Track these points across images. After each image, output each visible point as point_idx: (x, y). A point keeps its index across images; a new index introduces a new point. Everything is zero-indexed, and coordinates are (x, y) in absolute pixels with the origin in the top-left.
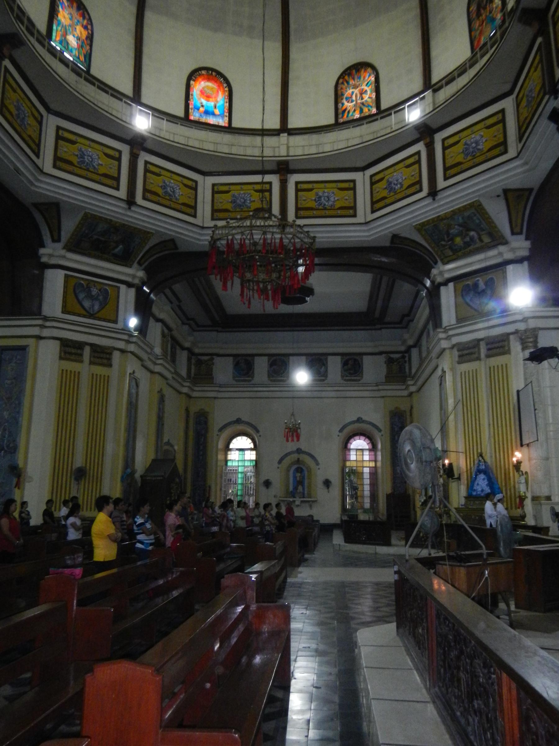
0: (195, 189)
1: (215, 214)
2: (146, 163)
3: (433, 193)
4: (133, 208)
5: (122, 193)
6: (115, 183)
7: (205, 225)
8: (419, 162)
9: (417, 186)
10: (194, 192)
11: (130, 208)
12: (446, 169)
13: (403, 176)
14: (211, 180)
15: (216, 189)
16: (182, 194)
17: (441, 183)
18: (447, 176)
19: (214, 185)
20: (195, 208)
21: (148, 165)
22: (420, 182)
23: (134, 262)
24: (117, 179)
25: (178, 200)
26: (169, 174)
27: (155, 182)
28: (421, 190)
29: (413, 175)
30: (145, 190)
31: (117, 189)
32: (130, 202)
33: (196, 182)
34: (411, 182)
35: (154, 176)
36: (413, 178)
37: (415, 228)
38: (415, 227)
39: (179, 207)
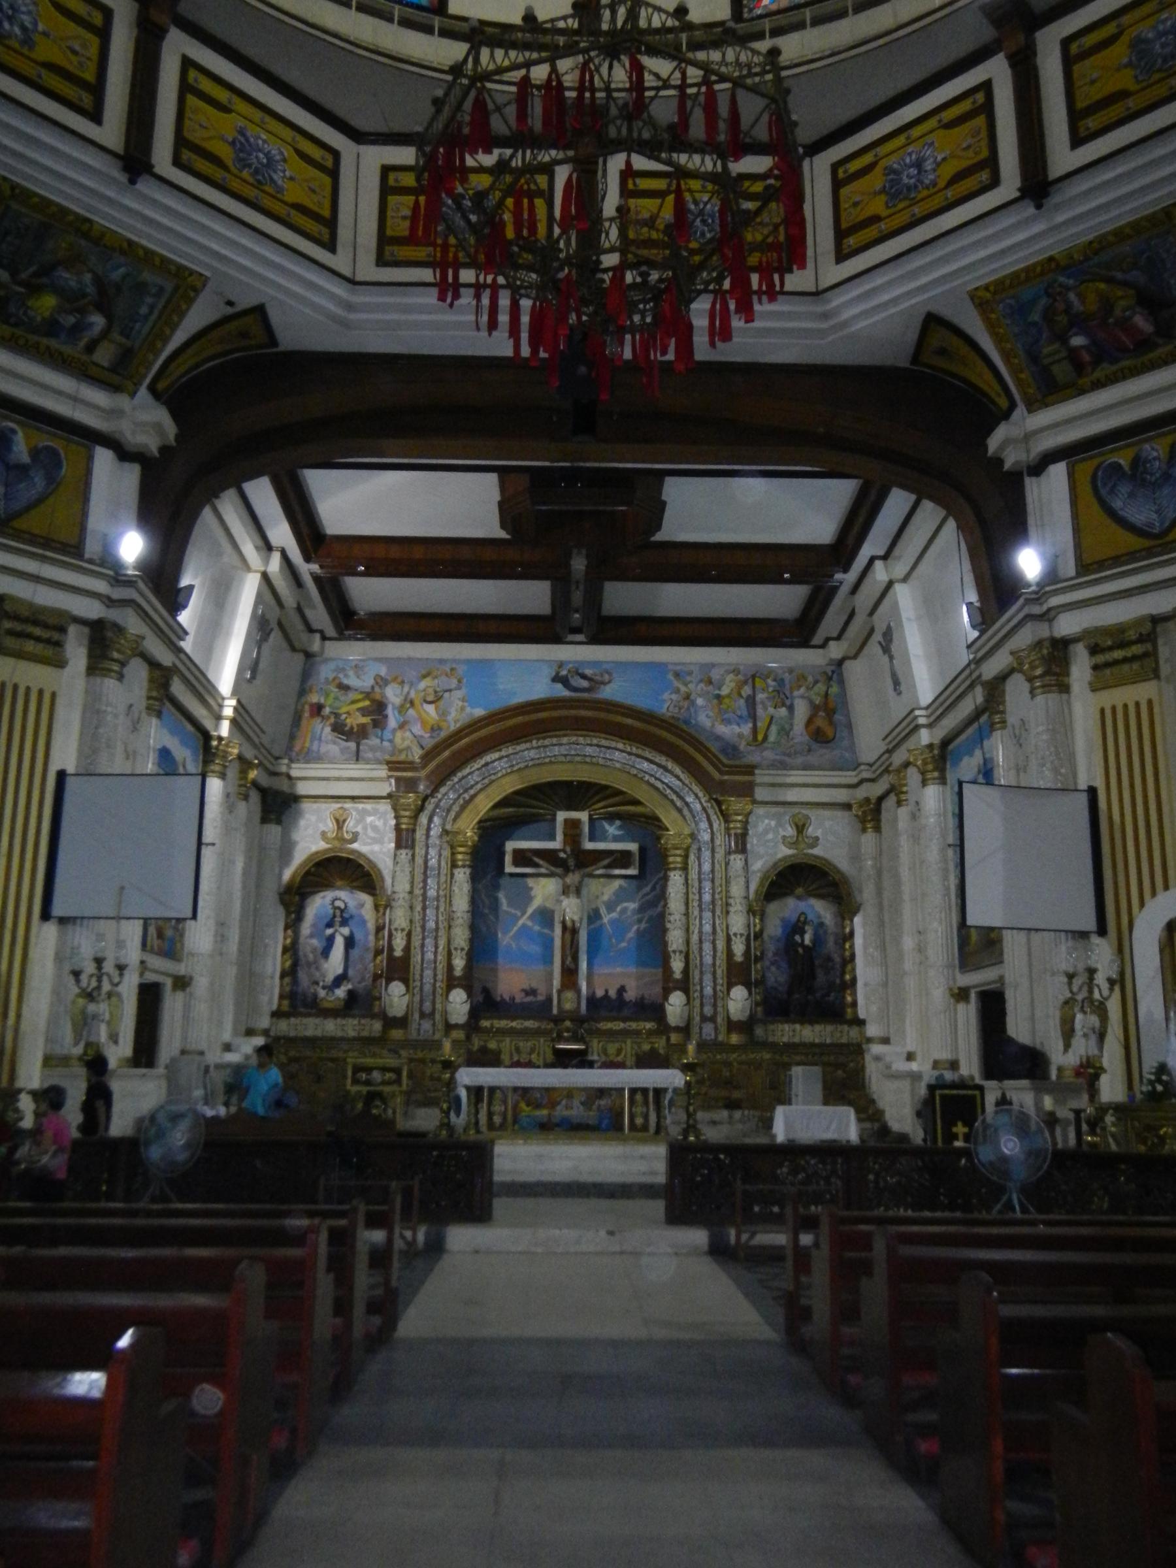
0: (334, 174)
1: (388, 249)
2: (187, 63)
3: (1038, 187)
4: (145, 186)
5: (111, 131)
6: (87, 100)
7: (360, 277)
8: (988, 109)
9: (984, 176)
10: (327, 180)
11: (132, 182)
12: (1075, 116)
13: (943, 153)
14: (377, 156)
15: (391, 182)
16: (295, 182)
17: (1062, 157)
18: (1083, 133)
19: (386, 170)
20: (331, 223)
21: (192, 74)
22: (991, 162)
23: (137, 385)
24: (97, 89)
25: (280, 190)
26: (257, 115)
27: (216, 129)
28: (995, 182)
29: (969, 147)
30: (181, 141)
31: (96, 117)
32: (135, 162)
33: (336, 154)
34: (965, 164)
35: (210, 110)
36: (970, 153)
37: (972, 298)
38: (973, 295)
39: (282, 210)
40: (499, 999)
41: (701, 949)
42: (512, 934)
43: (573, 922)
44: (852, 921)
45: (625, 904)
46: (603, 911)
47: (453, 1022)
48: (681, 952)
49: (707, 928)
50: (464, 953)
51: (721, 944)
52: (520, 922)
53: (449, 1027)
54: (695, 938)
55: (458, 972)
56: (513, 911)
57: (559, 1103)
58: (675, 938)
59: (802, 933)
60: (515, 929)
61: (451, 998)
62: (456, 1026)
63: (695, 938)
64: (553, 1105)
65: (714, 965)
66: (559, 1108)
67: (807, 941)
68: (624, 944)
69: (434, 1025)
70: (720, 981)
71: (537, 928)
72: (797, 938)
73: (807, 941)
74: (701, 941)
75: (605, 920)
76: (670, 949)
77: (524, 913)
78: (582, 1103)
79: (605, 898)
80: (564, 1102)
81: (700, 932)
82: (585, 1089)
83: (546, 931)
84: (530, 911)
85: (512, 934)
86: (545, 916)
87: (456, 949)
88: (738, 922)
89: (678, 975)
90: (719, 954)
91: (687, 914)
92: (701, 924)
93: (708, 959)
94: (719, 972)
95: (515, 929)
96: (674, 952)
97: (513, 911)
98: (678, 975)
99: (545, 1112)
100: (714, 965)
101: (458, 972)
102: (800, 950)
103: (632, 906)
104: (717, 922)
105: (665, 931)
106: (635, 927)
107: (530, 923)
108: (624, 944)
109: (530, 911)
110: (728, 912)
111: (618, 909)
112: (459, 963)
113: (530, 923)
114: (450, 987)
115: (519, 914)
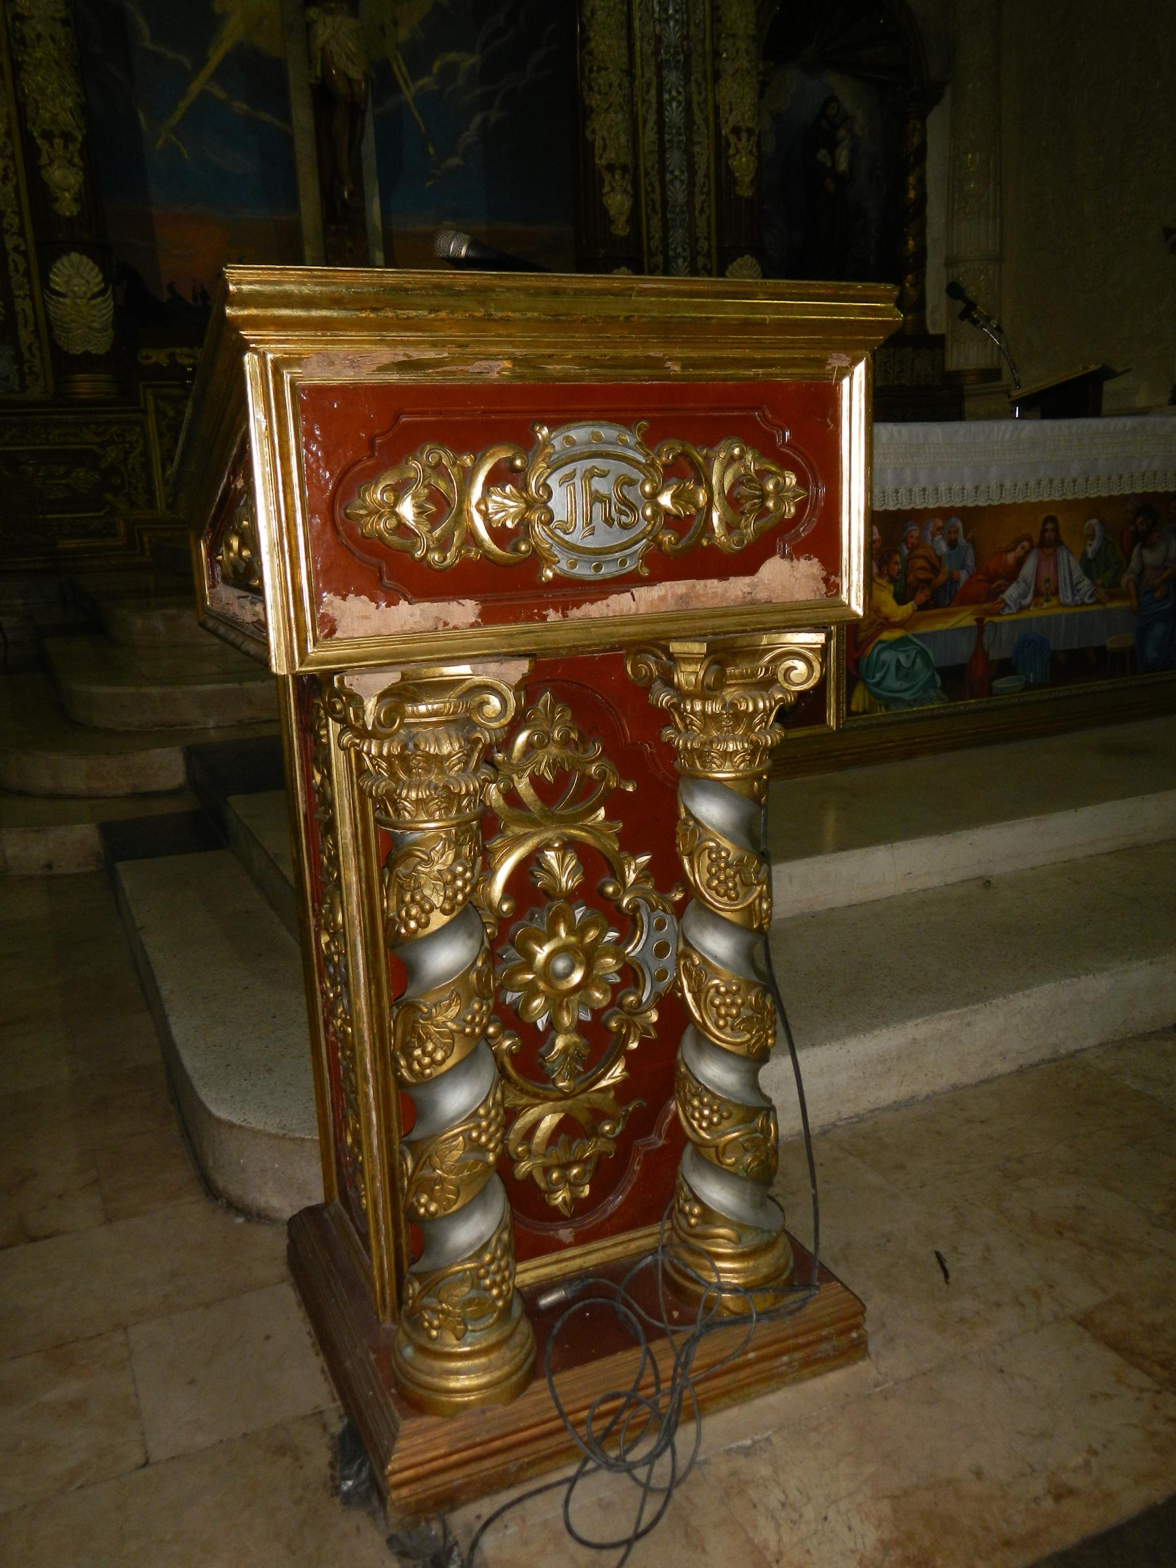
40: (166, 296)
41: (662, 169)
42: (174, 120)
43: (350, 81)
44: (923, 120)
45: (452, 56)
46: (400, 69)
47: (78, 350)
48: (624, 169)
49: (674, 113)
50: (74, 147)
51: (704, 156)
52: (195, 87)
53: (66, 364)
54: (649, 136)
55: (67, 206)
56: (170, 55)
57: (1012, 575)
58: (608, 132)
59: (832, 148)
60: (183, 105)
61: (57, 282)
62: (88, 361)
63: (649, 136)
64: (990, 585)
65: (690, 204)
66: (1011, 593)
67: (843, 165)
68: (456, 161)
69: (18, 359)
70: (703, 245)
71: (241, 107)
72: (822, 155)
73: (843, 165)
74: (662, 149)
75: (408, 94)
76: (600, 162)
77: (200, 62)
78: (1088, 567)
79: (403, 34)
80: (1029, 569)
81: (661, 124)
82: (1095, 506)
83: (266, 117)
84: (215, 57)
85: (174, 120)
86: (258, 74)
87: (48, 135)
88: (738, 100)
89: (620, 229)
90: (700, 178)
91: (630, 72)
92: (660, 110)
93: (678, 194)
94: (701, 222)
95: (183, 105)
96: (610, 168)
97: (170, 55)
98: (620, 229)
99: (965, 618)
100: (690, 204)
101: (67, 206)
102: (830, 185)
103: (469, 61)
104: (696, 98)
105: (580, 114)
106: (478, 119)
107: (219, 93)
108: (456, 161)
109: (215, 57)
110: (717, 76)
111: (436, 68)
112: (64, 178)
113: (219, 93)
114: (48, 251)
115: (189, 66)
